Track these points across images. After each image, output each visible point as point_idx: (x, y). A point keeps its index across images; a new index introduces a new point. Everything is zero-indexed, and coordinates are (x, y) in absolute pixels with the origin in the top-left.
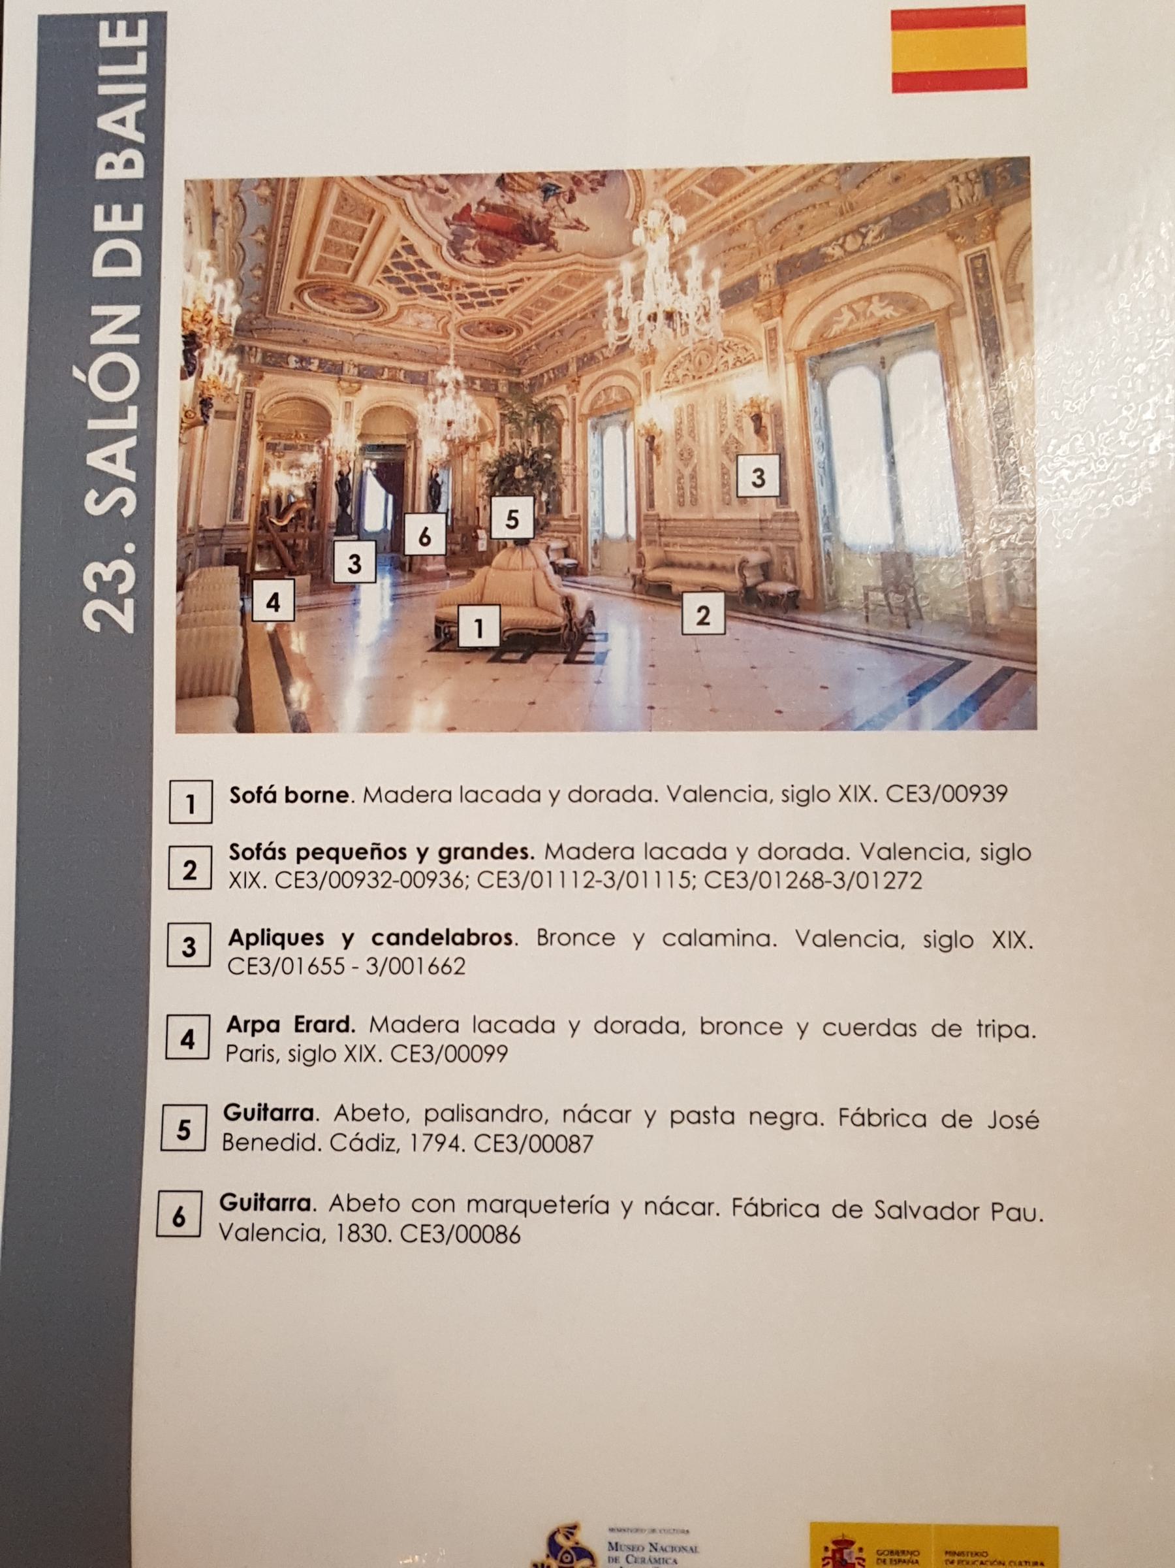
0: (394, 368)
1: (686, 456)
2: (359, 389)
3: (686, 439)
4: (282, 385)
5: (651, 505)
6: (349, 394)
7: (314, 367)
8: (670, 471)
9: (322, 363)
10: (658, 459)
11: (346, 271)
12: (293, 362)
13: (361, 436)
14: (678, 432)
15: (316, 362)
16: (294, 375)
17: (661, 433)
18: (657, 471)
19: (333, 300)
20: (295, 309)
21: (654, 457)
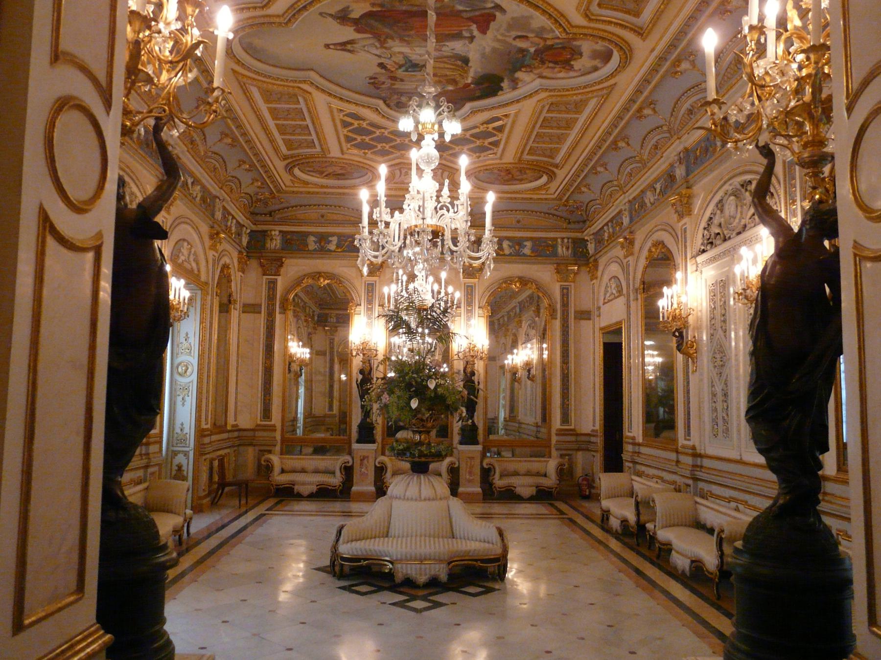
7: (332, 247)
10: (693, 362)
12: (311, 241)
15: (335, 240)
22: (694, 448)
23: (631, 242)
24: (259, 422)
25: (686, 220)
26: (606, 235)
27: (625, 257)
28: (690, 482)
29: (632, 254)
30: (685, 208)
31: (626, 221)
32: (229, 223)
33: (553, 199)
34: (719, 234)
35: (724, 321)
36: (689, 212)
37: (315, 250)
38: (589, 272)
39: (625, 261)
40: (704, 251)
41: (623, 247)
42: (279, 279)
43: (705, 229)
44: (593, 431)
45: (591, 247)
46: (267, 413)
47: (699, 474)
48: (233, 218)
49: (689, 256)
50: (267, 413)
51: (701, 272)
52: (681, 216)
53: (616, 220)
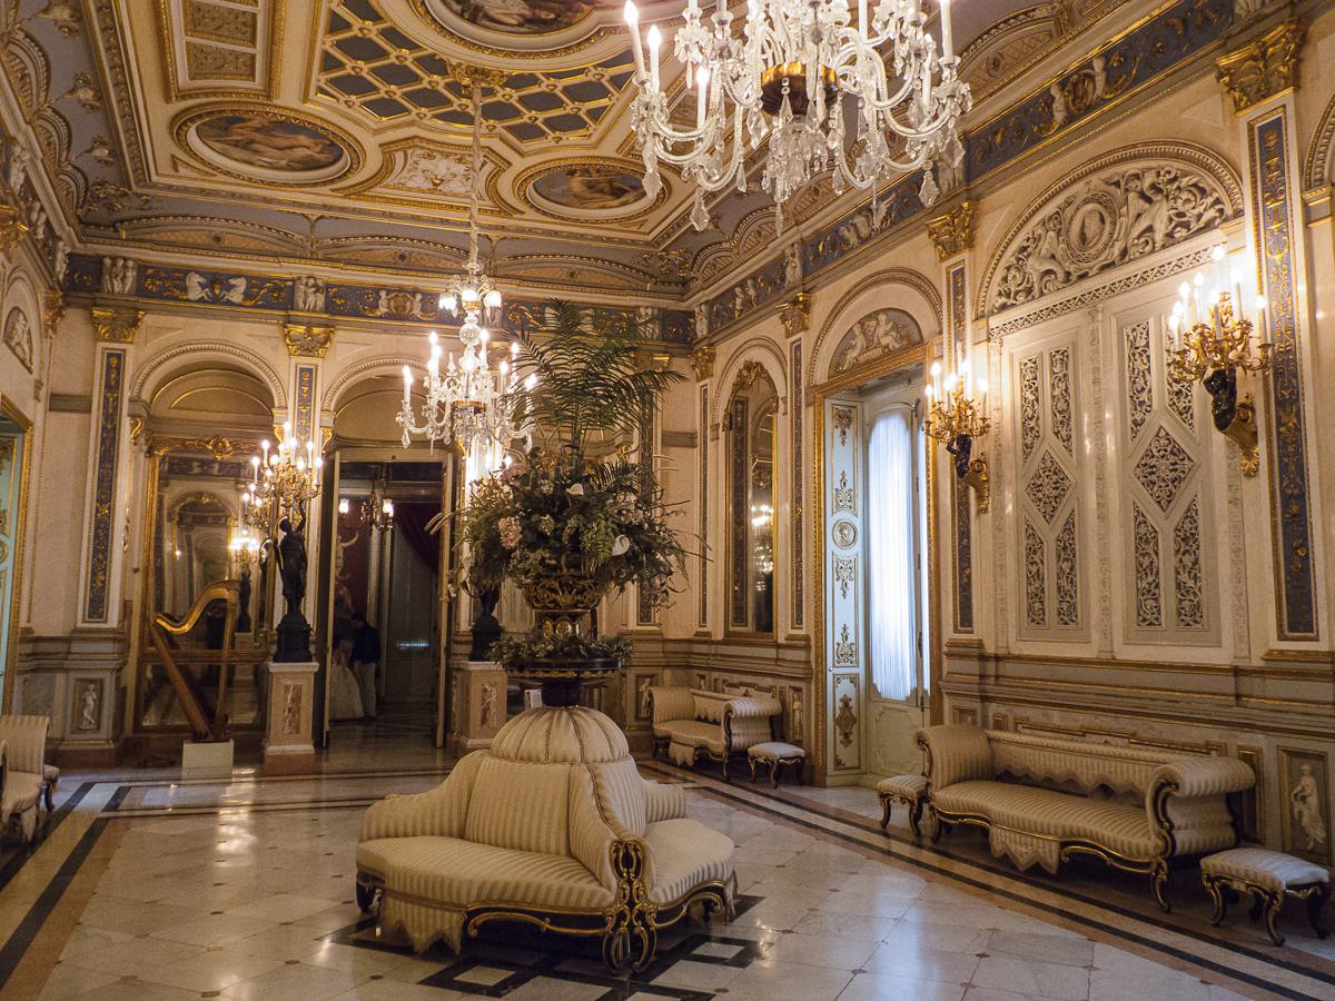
0: (401, 289)
1: (1051, 488)
2: (327, 339)
3: (1050, 444)
4: (174, 336)
5: (965, 617)
6: (308, 350)
8: (1010, 537)
9: (255, 282)
10: (980, 498)
11: (252, 76)
13: (337, 444)
14: (1029, 427)
16: (204, 315)
17: (984, 430)
18: (979, 528)
19: (247, 145)
20: (183, 171)
21: (972, 490)
22: (980, 644)
23: (807, 307)
24: (80, 625)
25: (965, 254)
26: (738, 301)
27: (788, 335)
28: (977, 705)
29: (806, 329)
30: (958, 237)
31: (793, 273)
32: (34, 216)
33: (647, 244)
34: (1049, 272)
35: (1065, 422)
36: (970, 243)
37: (202, 300)
38: (693, 367)
39: (786, 346)
40: (1004, 307)
41: (783, 319)
42: (130, 349)
43: (1008, 269)
44: (698, 634)
45: (701, 327)
46: (97, 605)
47: (991, 689)
48: (42, 209)
49: (969, 315)
50: (97, 605)
51: (1001, 343)
52: (950, 249)
53: (772, 276)
